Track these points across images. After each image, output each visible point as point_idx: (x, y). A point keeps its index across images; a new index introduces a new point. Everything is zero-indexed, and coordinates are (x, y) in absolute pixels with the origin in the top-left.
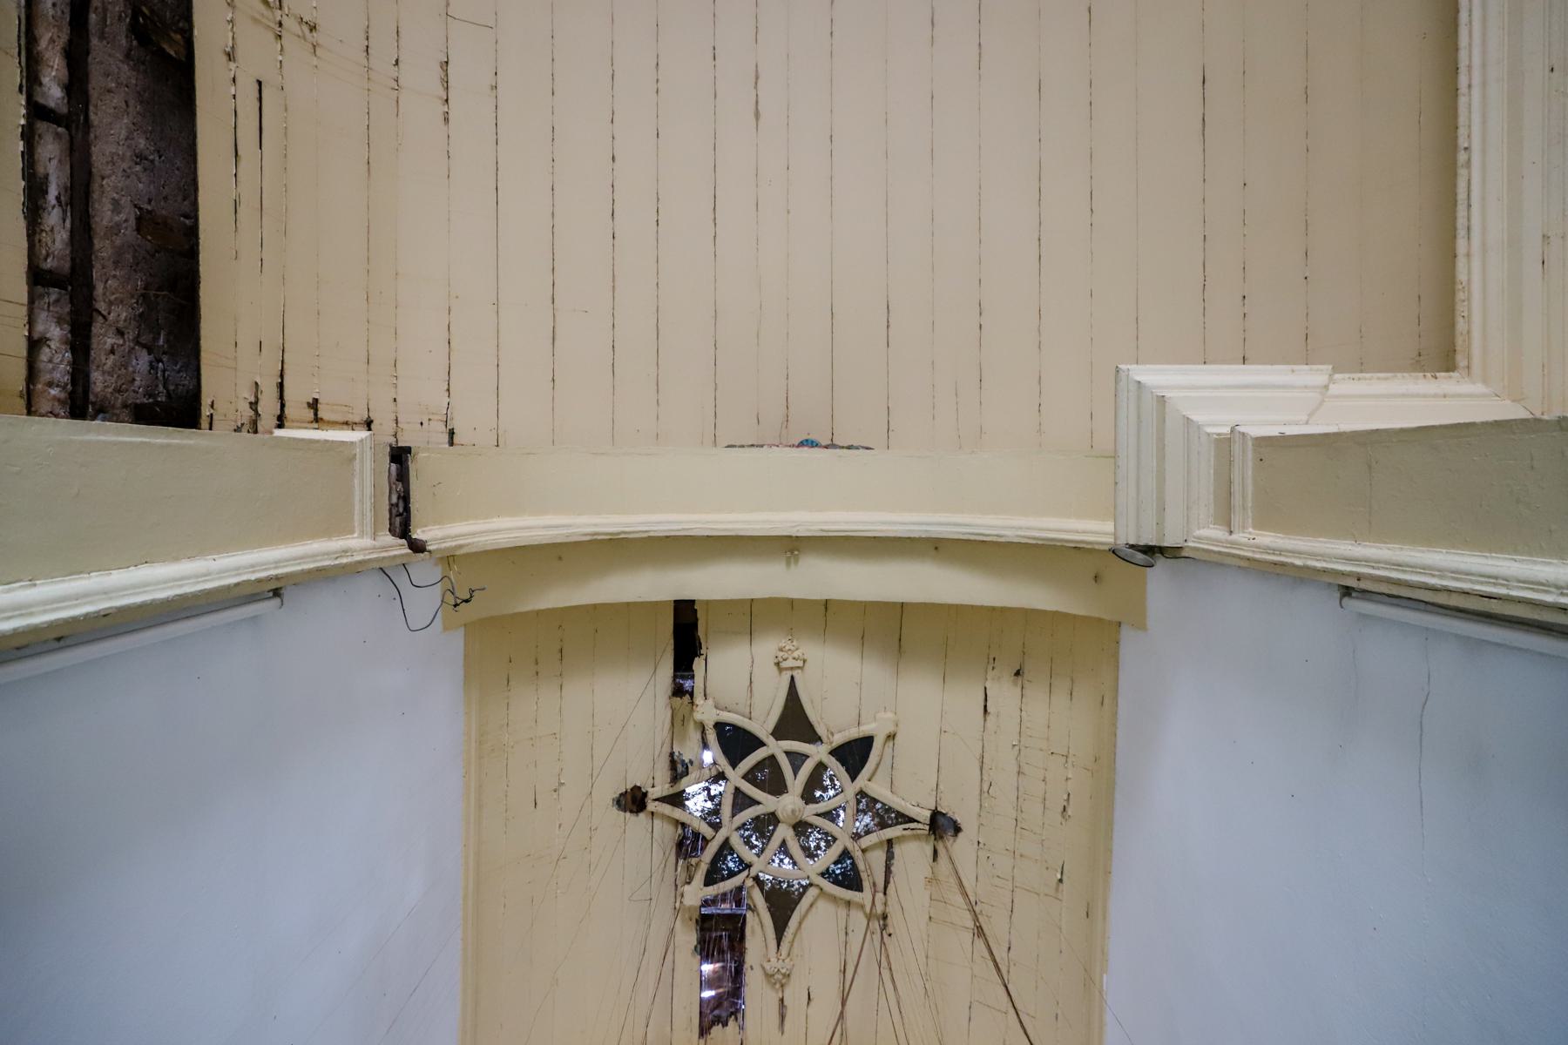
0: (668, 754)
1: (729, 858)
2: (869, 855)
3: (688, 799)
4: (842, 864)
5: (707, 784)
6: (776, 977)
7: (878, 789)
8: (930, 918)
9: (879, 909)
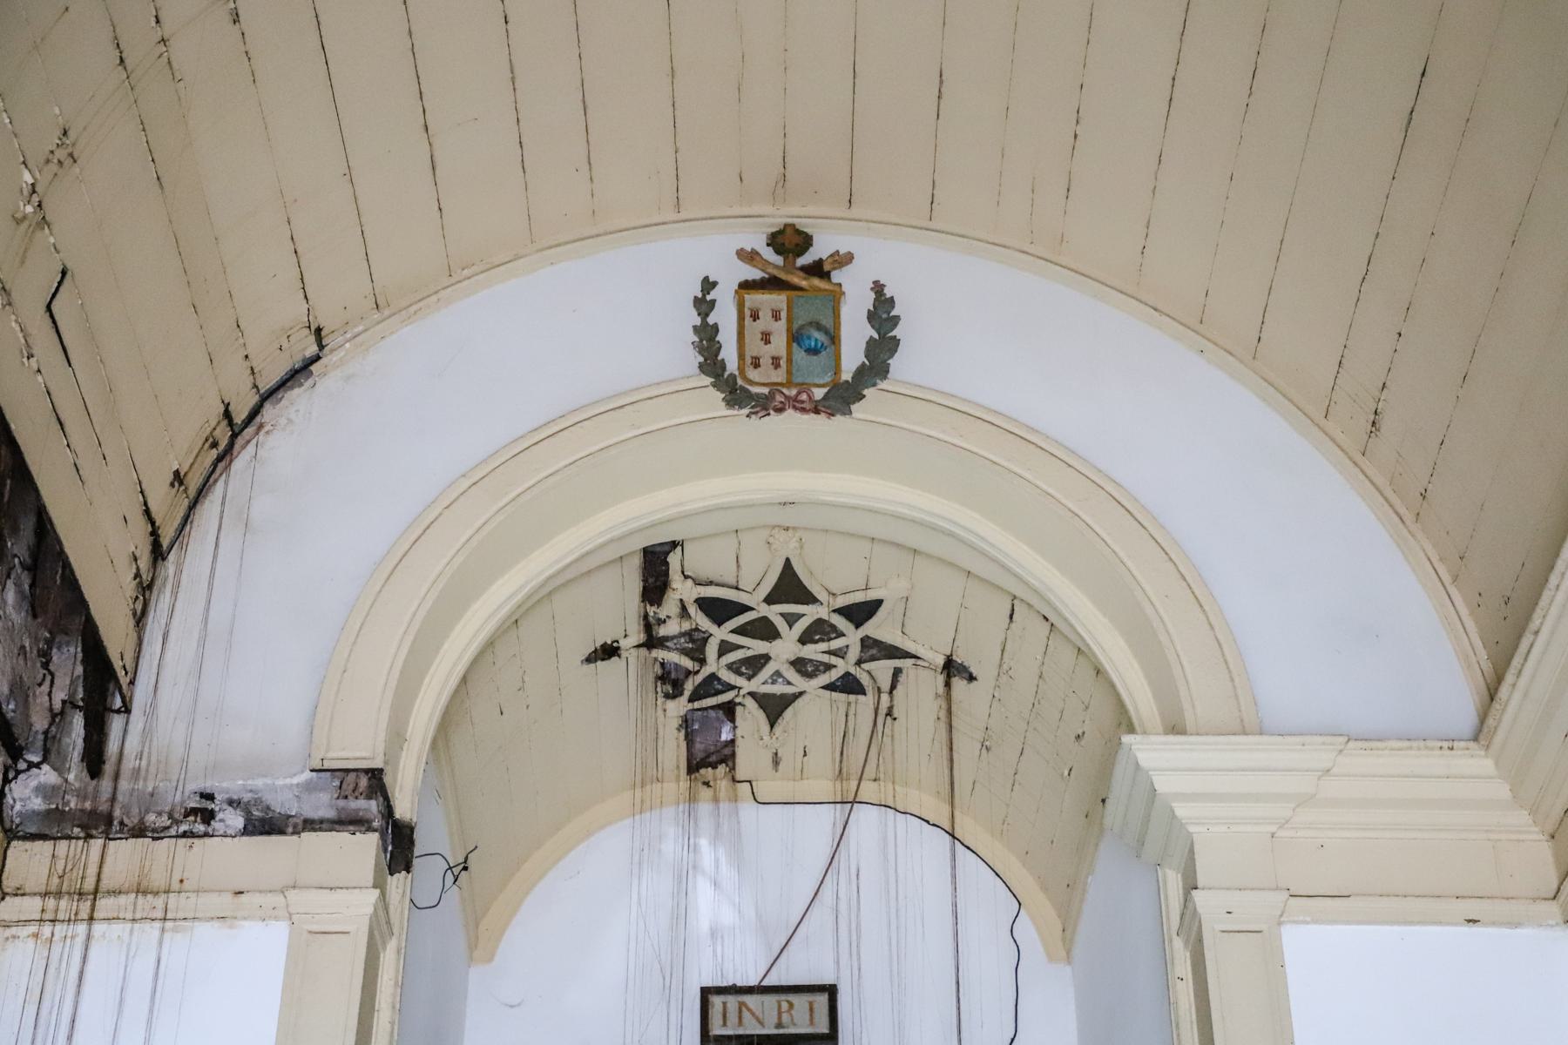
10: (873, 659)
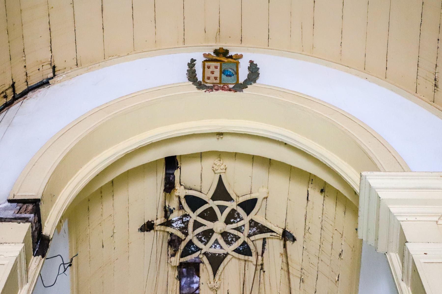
3: (173, 223)
4: (243, 246)
5: (181, 217)
7: (260, 219)
9: (260, 262)
10: (255, 234)
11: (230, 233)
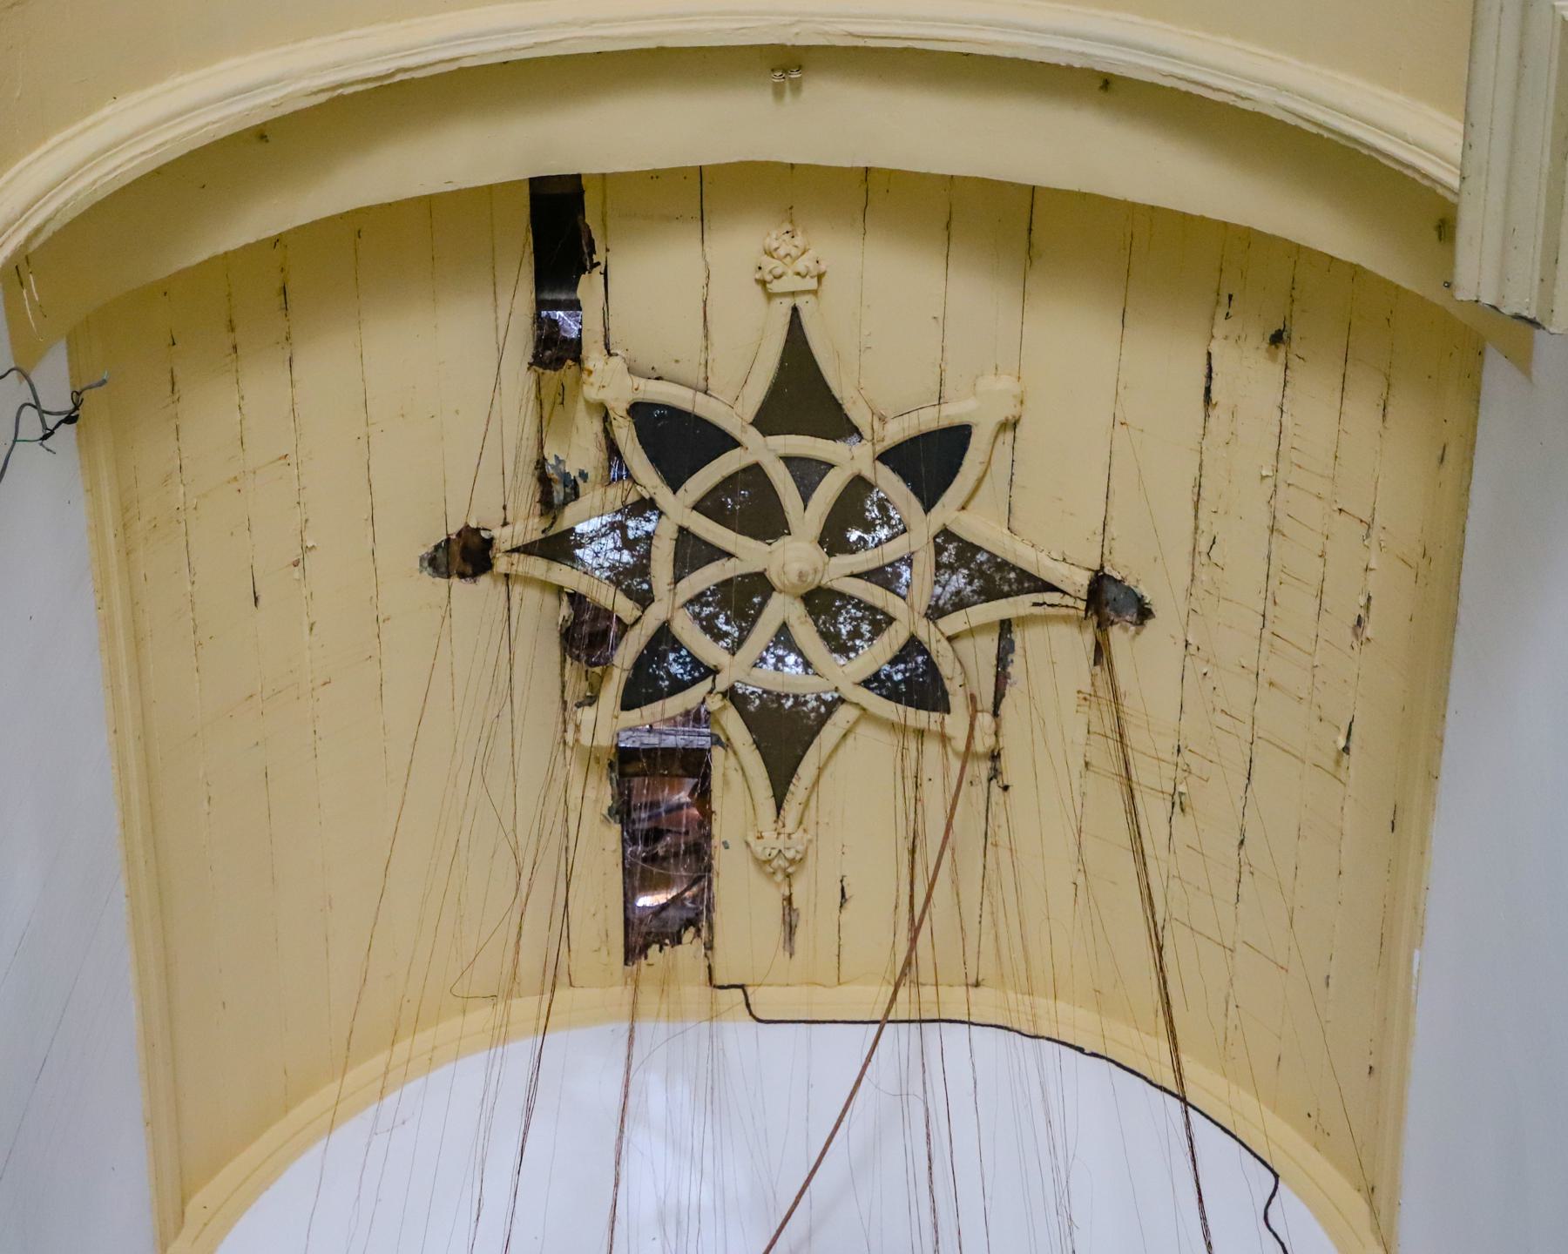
0: (533, 466)
1: (672, 656)
2: (964, 646)
3: (581, 546)
4: (906, 662)
5: (619, 517)
6: (775, 864)
8: (1087, 764)
9: (983, 743)
11: (846, 598)
